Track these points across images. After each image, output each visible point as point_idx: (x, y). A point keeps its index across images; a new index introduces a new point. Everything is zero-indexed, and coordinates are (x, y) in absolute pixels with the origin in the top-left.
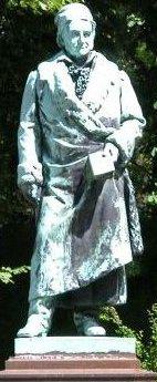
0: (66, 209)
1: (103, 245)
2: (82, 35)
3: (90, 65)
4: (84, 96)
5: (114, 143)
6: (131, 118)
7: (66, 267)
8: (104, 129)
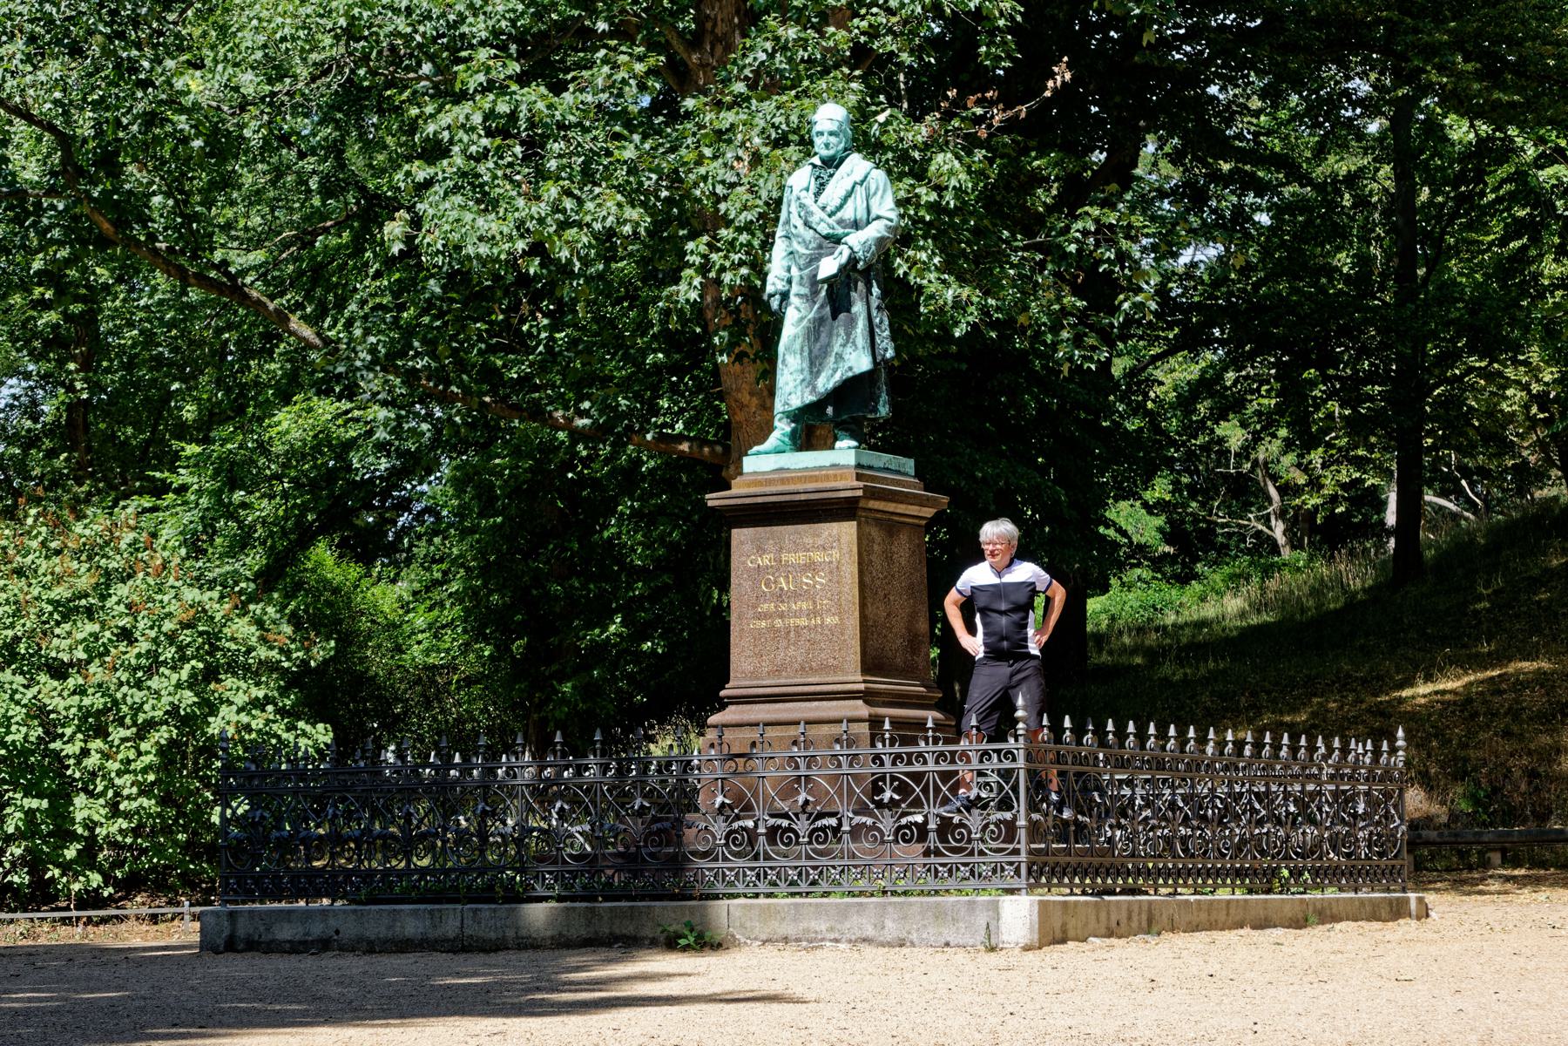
6: (878, 218)
8: (840, 231)
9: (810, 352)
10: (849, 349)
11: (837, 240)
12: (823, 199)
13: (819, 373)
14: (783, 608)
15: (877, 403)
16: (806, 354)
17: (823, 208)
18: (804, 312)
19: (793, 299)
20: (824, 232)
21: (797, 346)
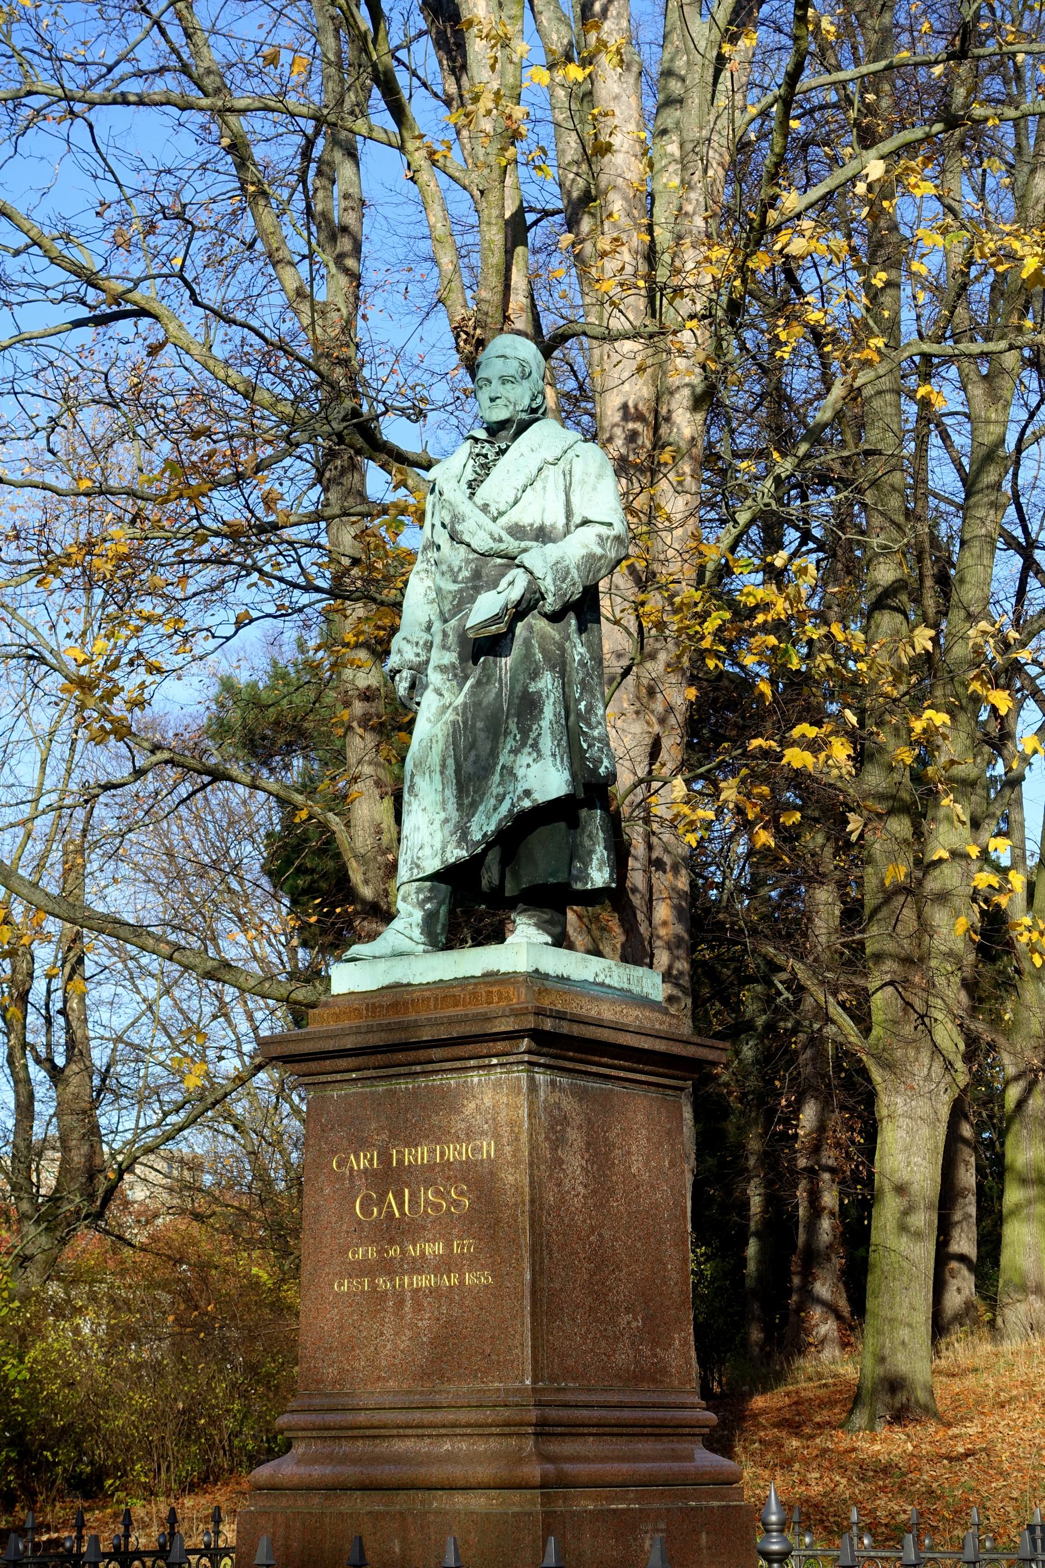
1: (503, 767)
6: (585, 522)
7: (446, 821)
8: (511, 544)
9: (458, 772)
10: (525, 758)
11: (511, 560)
12: (484, 492)
13: (474, 806)
14: (394, 1252)
15: (587, 864)
16: (450, 771)
17: (485, 508)
19: (434, 678)
20: (481, 542)
21: (434, 759)
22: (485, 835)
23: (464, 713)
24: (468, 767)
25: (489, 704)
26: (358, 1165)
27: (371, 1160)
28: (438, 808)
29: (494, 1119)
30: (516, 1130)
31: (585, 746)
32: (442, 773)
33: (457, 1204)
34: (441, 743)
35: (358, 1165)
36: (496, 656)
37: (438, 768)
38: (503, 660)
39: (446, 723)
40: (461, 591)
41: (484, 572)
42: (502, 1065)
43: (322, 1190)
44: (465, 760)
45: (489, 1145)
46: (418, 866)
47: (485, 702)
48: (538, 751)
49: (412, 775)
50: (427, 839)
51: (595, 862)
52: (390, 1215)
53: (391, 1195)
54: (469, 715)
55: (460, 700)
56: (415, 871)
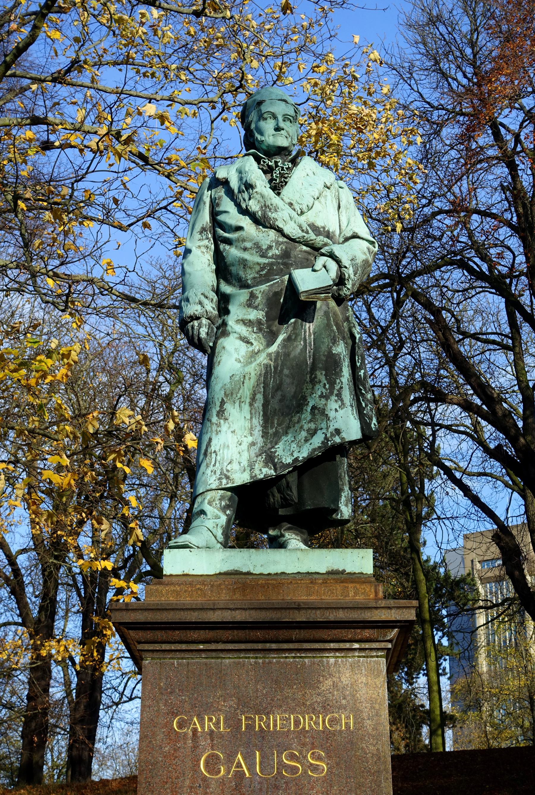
0: (254, 354)
1: (314, 408)
2: (280, 118)
3: (294, 162)
4: (286, 191)
5: (332, 256)
6: (355, 236)
7: (253, 444)
9: (265, 405)
10: (333, 404)
18: (257, 346)
21: (246, 391)
22: (296, 460)
23: (276, 360)
24: (274, 404)
25: (295, 356)
26: (203, 727)
27: (218, 722)
28: (246, 433)
29: (354, 696)
30: (377, 706)
31: (364, 405)
32: (251, 405)
33: (315, 768)
34: (253, 381)
35: (203, 727)
36: (303, 320)
37: (248, 400)
38: (308, 325)
39: (260, 365)
40: (271, 264)
41: (293, 253)
42: (360, 649)
43: (161, 747)
44: (272, 397)
45: (348, 718)
46: (227, 477)
47: (292, 356)
48: (342, 401)
49: (223, 403)
50: (236, 456)
51: (343, 499)
52: (240, 775)
53: (239, 756)
54: (280, 362)
55: (274, 348)
56: (224, 481)
